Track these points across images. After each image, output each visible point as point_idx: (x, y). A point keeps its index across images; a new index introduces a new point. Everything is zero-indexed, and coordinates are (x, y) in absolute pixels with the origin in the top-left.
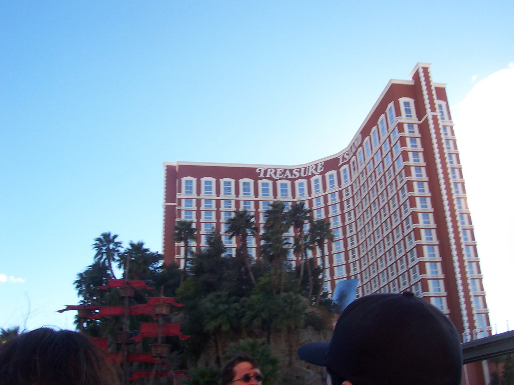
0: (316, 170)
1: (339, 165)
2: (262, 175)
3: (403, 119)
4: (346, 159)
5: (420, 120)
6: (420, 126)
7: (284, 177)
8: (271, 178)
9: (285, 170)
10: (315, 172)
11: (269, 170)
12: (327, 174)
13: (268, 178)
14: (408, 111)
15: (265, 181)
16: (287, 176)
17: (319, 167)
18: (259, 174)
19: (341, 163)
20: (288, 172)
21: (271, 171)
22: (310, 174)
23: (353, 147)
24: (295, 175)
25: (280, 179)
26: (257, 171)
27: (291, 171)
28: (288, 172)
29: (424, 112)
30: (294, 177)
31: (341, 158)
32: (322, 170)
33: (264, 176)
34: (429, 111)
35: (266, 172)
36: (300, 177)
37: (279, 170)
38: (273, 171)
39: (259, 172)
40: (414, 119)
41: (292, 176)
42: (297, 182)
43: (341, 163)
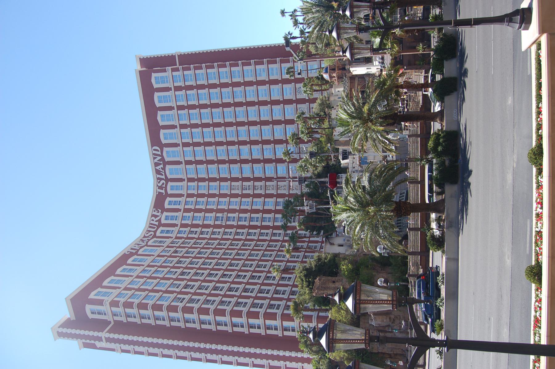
0: (156, 216)
1: (164, 194)
2: (134, 251)
4: (163, 184)
12: (167, 206)
17: (156, 213)
19: (163, 191)
22: (157, 223)
25: (147, 243)
27: (145, 237)
30: (151, 236)
32: (160, 211)
36: (155, 232)
43: (163, 191)
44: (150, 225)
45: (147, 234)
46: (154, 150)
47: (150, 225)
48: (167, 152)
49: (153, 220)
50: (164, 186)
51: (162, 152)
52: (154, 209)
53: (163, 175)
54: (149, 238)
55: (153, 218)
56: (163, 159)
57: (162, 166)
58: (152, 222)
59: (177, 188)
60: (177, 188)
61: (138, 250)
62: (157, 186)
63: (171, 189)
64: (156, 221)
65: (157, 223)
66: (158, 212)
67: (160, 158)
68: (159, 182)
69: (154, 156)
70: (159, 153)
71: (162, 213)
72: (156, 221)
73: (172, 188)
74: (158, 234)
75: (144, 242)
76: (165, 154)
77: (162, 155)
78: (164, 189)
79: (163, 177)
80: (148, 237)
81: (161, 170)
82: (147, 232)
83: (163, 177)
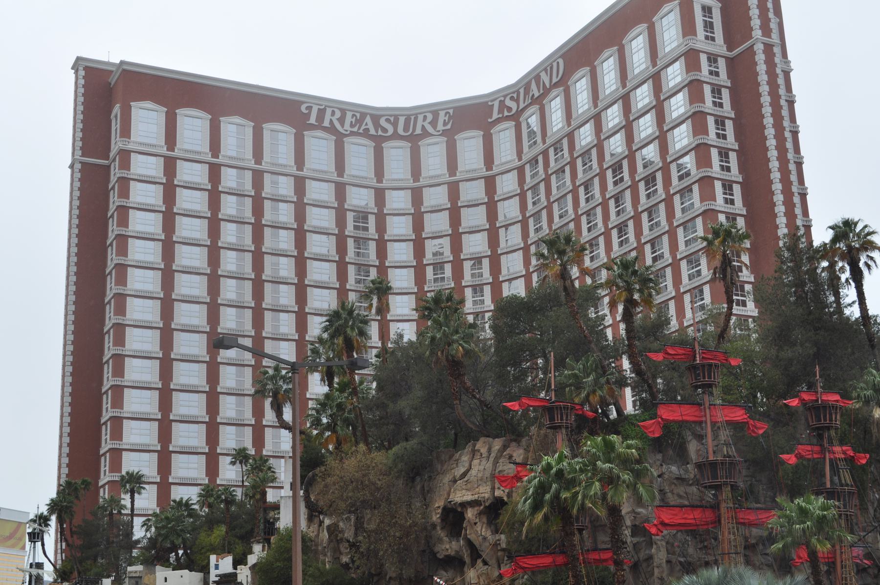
0: (434, 123)
1: (490, 120)
2: (313, 120)
3: (700, 40)
5: (730, 49)
6: (730, 61)
7: (361, 131)
8: (332, 130)
9: (363, 115)
10: (430, 129)
11: (329, 112)
13: (325, 129)
14: (709, 26)
15: (319, 133)
16: (367, 130)
17: (442, 117)
18: (308, 116)
19: (495, 116)
20: (368, 120)
21: (333, 113)
22: (418, 131)
23: (533, 86)
24: (385, 130)
25: (352, 134)
26: (303, 108)
27: (376, 119)
28: (368, 120)
29: (747, 33)
30: (380, 133)
31: (496, 104)
32: (449, 127)
33: (317, 124)
34: (757, 33)
35: (321, 113)
36: (396, 136)
37: (349, 115)
38: (338, 114)
39: (307, 112)
40: (719, 46)
41: (377, 132)
43: (495, 116)
44: (413, 118)
47: (413, 118)
50: (506, 114)
52: (451, 111)
54: (372, 132)
57: (537, 94)
61: (319, 126)
62: (505, 96)
65: (418, 131)
66: (445, 124)
69: (549, 68)
71: (444, 133)
78: (500, 116)
79: (522, 106)
81: (531, 95)
82: (392, 119)
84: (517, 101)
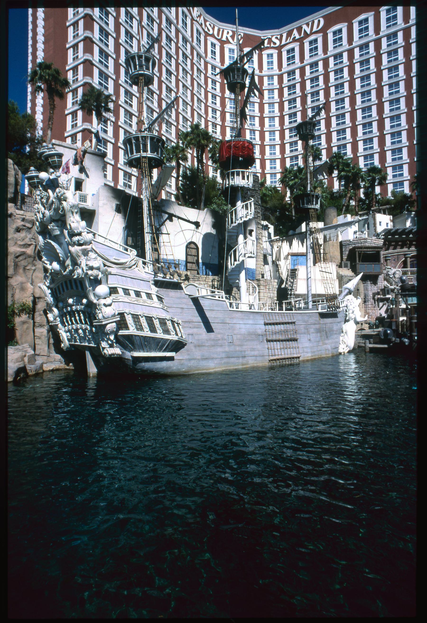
4: (275, 43)
16: (202, 24)
22: (224, 39)
24: (209, 30)
25: (196, 21)
30: (206, 30)
36: (213, 36)
42: (210, 40)
44: (221, 30)
45: (210, 25)
46: (319, 21)
48: (316, 41)
49: (228, 33)
51: (316, 32)
53: (287, 39)
54: (203, 26)
55: (231, 33)
56: (307, 35)
57: (298, 37)
58: (225, 32)
59: (270, 63)
60: (270, 63)
63: (268, 55)
64: (227, 37)
65: (224, 39)
67: (308, 32)
68: (277, 38)
70: (315, 29)
72: (227, 37)
73: (270, 56)
74: (210, 40)
75: (197, 17)
76: (312, 37)
77: (312, 33)
78: (269, 46)
79: (283, 42)
80: (206, 26)
81: (292, 37)
82: (212, 25)
83: (283, 42)
84: (281, 40)
